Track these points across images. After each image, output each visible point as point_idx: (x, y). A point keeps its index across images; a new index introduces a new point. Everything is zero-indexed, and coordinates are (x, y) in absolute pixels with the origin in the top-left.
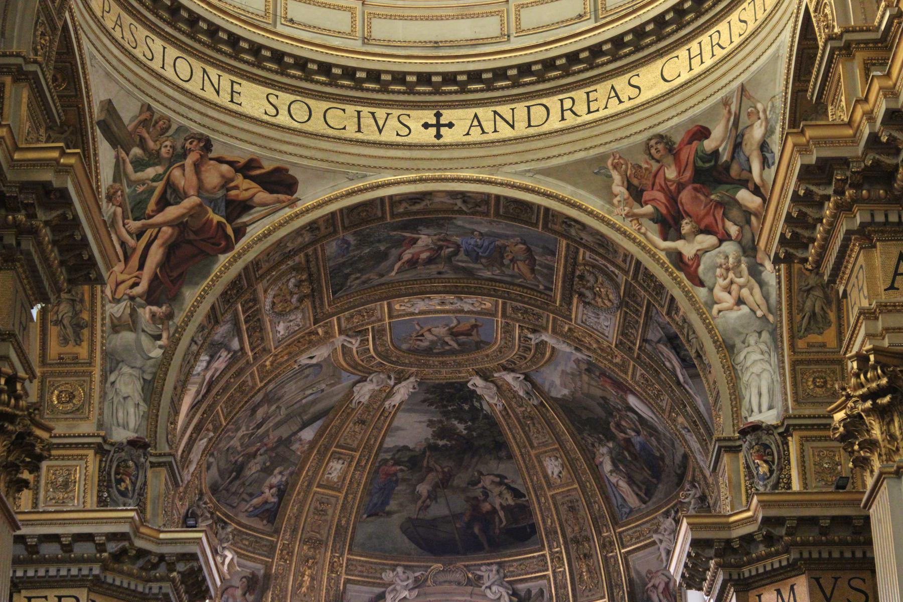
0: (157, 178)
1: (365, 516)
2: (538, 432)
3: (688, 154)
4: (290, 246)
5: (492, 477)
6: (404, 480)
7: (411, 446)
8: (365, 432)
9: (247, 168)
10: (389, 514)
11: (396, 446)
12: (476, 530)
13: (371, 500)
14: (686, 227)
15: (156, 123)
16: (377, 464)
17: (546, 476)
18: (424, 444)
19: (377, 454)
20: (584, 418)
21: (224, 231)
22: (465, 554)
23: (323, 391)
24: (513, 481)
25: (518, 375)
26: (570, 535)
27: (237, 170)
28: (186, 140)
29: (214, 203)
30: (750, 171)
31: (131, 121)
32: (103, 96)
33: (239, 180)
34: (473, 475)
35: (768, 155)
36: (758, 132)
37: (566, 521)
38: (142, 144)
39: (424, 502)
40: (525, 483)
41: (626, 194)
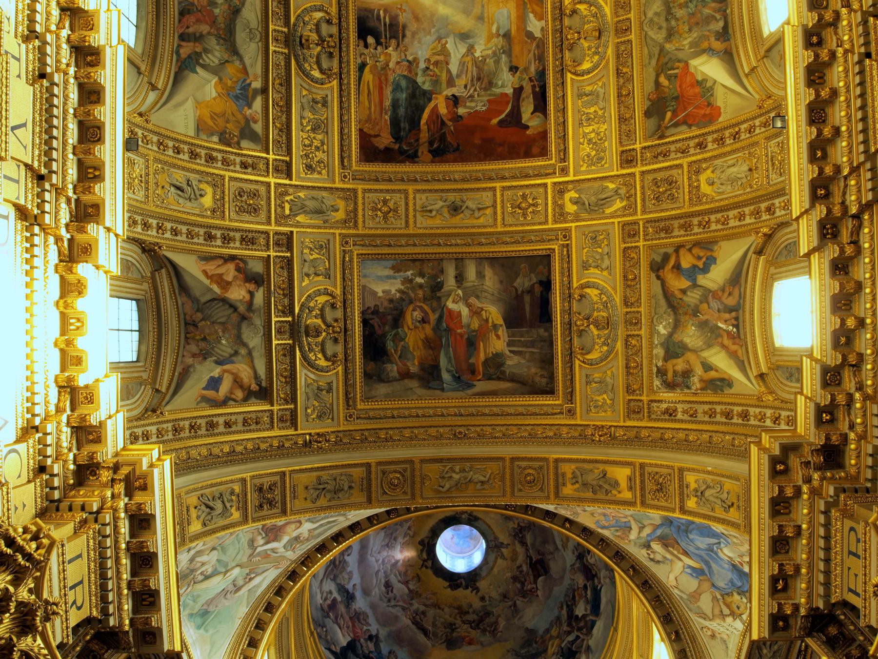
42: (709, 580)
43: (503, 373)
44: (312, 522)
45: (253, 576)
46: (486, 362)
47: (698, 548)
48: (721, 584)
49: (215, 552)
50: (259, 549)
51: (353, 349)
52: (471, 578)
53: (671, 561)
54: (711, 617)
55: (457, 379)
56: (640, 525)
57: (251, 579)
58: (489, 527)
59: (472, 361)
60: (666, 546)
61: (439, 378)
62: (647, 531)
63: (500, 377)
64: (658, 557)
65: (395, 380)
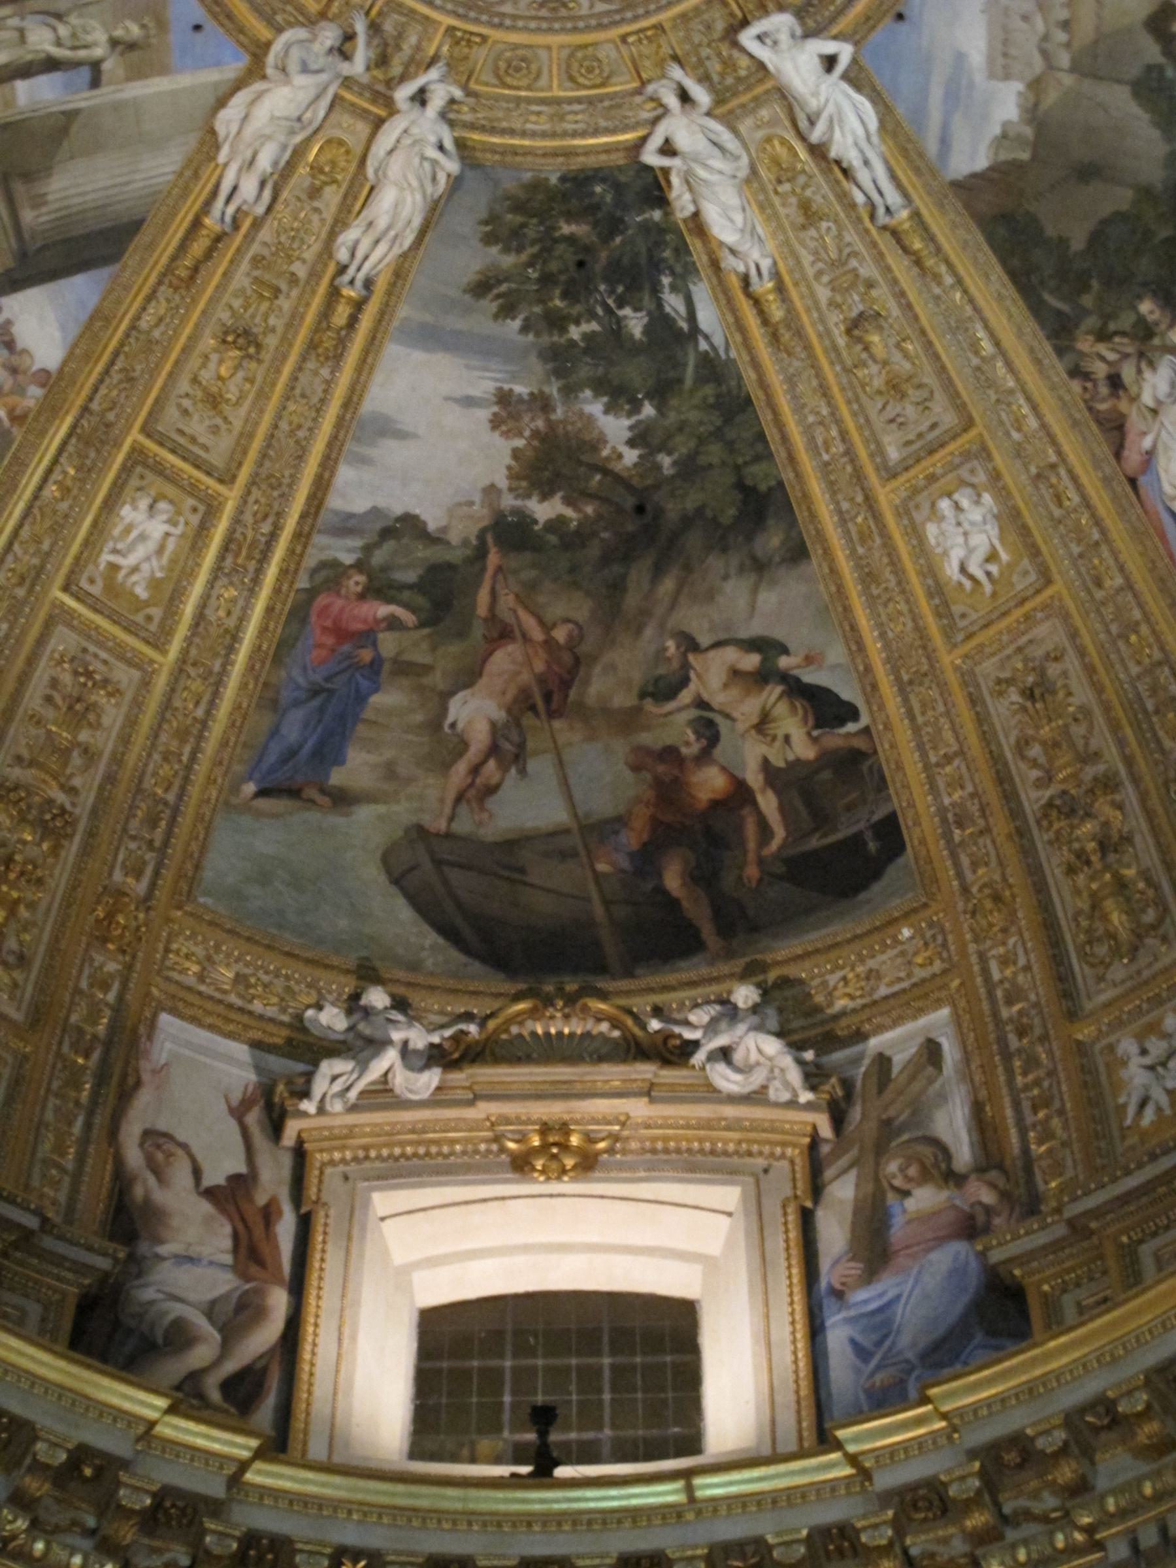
1: (250, 788)
2: (895, 388)
5: (731, 655)
6: (404, 668)
7: (433, 520)
8: (263, 395)
10: (343, 799)
11: (375, 512)
12: (673, 881)
13: (275, 732)
16: (303, 582)
17: (938, 590)
18: (481, 514)
19: (301, 536)
20: (1078, 243)
22: (629, 974)
23: (96, 66)
24: (809, 660)
25: (830, 47)
26: (1033, 799)
34: (660, 653)
37: (1022, 746)
39: (475, 770)
40: (857, 646)
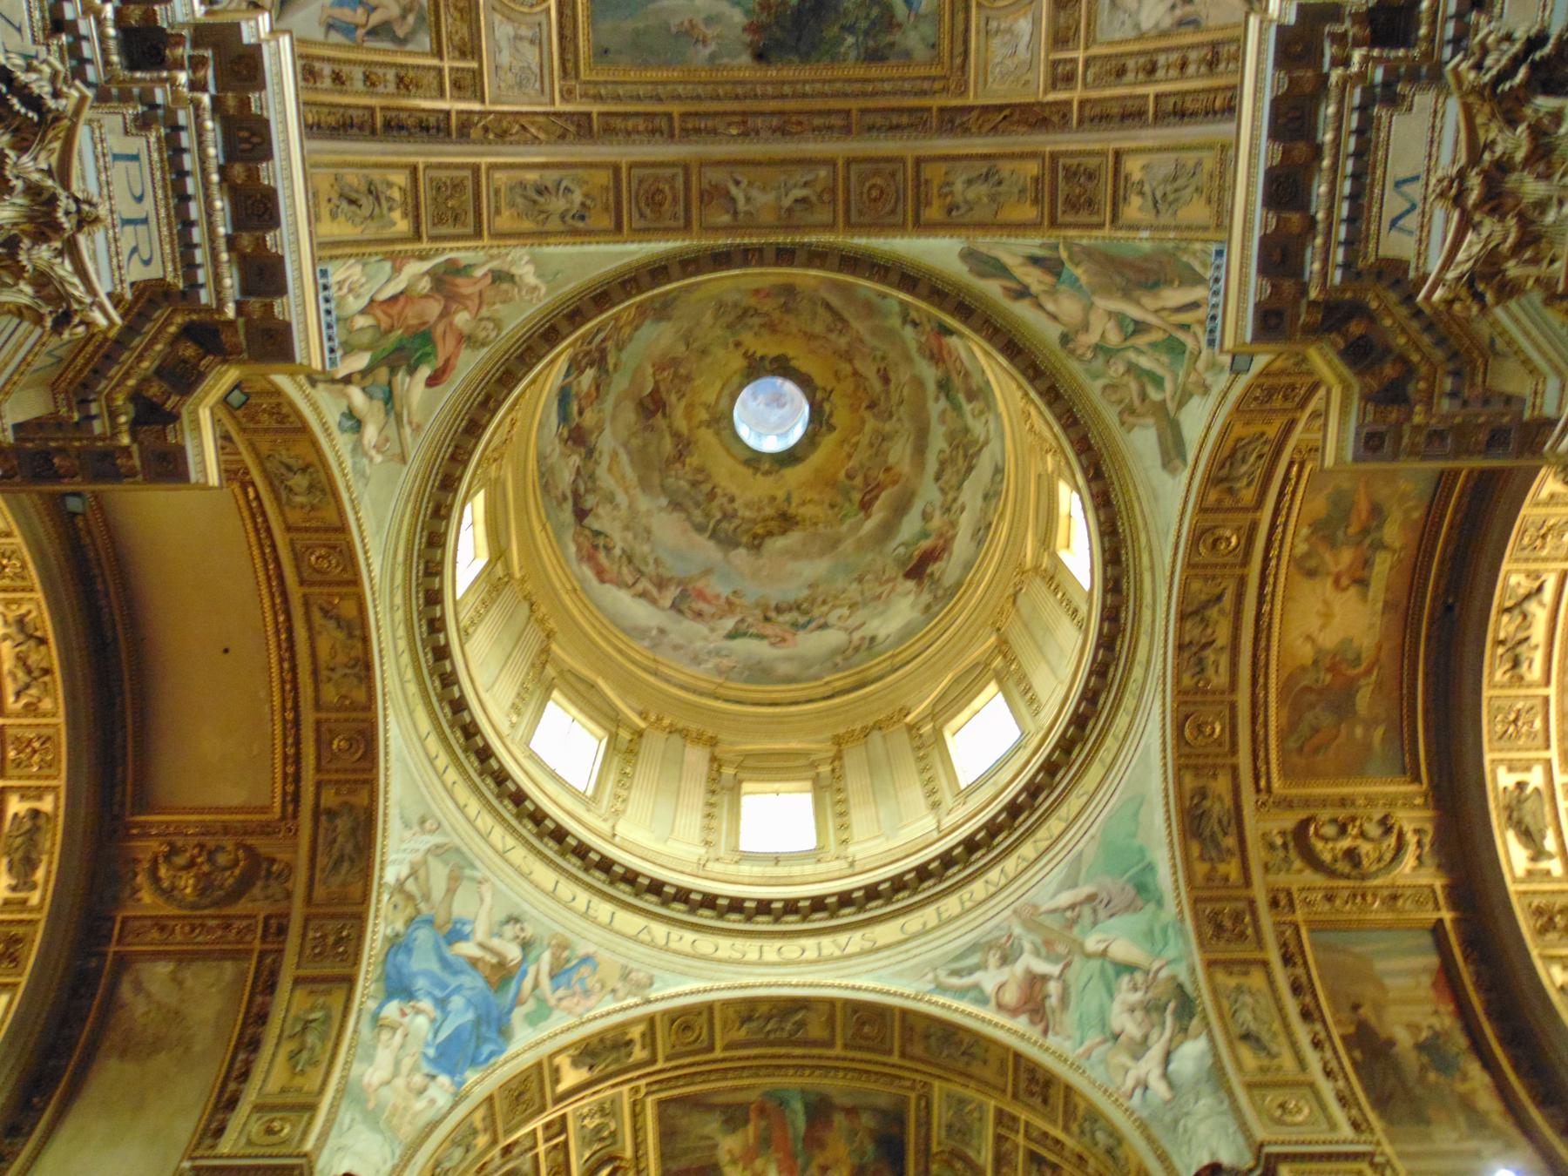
0: (1139, 351)
3: (444, 350)
4: (982, 189)
9: (1022, 293)
14: (425, 285)
15: (1121, 402)
21: (1071, 258)
27: (1036, 297)
28: (1090, 361)
29: (1075, 281)
30: (364, 389)
31: (1145, 427)
32: (1165, 476)
33: (1035, 288)
35: (348, 423)
36: (371, 433)
38: (1144, 396)
41: (515, 270)
42: (440, 928)
43: (724, 1113)
44: (982, 991)
45: (1069, 914)
46: (747, 1121)
47: (458, 989)
48: (423, 935)
49: (1116, 1027)
50: (1054, 970)
51: (917, 1164)
52: (755, 369)
53: (492, 934)
54: (430, 859)
55: (783, 1103)
56: (537, 992)
57: (1072, 907)
58: (727, 450)
59: (763, 1123)
60: (502, 964)
61: (807, 1106)
62: (528, 983)
63: (726, 1107)
64: (509, 930)
65: (866, 1108)
